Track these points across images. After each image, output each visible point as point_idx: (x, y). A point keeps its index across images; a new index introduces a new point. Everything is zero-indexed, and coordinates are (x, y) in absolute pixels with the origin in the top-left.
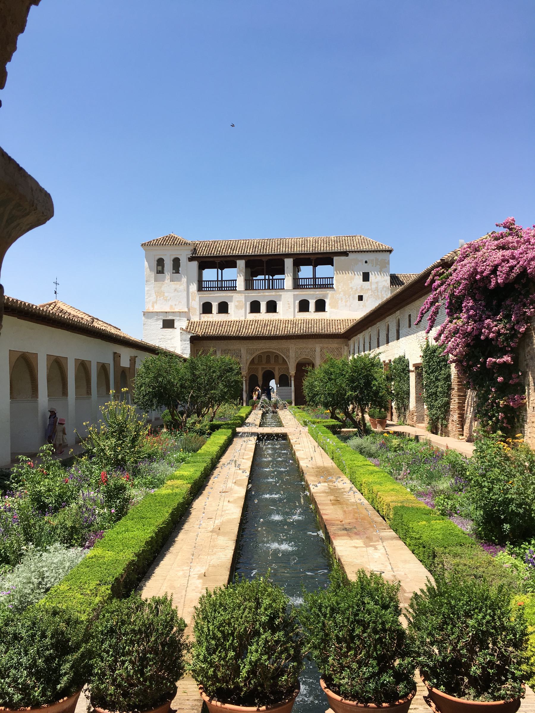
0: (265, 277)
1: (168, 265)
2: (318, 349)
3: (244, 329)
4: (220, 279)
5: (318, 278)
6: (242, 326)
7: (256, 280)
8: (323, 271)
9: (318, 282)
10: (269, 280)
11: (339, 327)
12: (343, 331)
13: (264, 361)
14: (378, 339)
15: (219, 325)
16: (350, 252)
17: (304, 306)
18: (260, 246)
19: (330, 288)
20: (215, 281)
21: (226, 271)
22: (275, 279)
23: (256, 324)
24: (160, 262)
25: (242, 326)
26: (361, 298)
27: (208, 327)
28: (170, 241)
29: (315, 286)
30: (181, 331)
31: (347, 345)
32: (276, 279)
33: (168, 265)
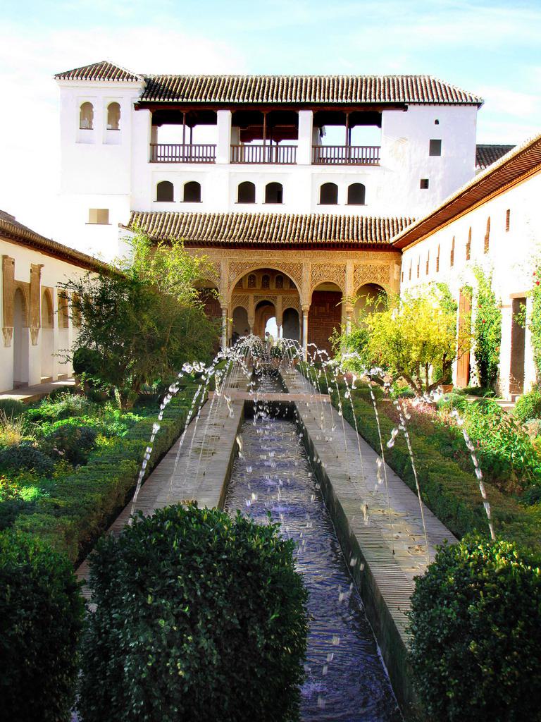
0: (265, 143)
1: (100, 114)
2: (350, 269)
3: (227, 229)
4: (187, 142)
5: (355, 147)
6: (223, 224)
7: (249, 146)
8: (363, 134)
9: (355, 154)
10: (271, 147)
11: (387, 232)
12: (392, 240)
13: (259, 286)
14: (452, 252)
15: (184, 221)
16: (410, 103)
17: (328, 194)
18: (257, 87)
19: (374, 165)
20: (179, 145)
21: (198, 129)
22: (280, 146)
23: (247, 221)
24: (87, 108)
25: (223, 224)
26: (425, 184)
27: (165, 224)
28: (104, 71)
29: (349, 161)
30: (121, 229)
31: (399, 263)
32: (284, 147)
33: (100, 114)
